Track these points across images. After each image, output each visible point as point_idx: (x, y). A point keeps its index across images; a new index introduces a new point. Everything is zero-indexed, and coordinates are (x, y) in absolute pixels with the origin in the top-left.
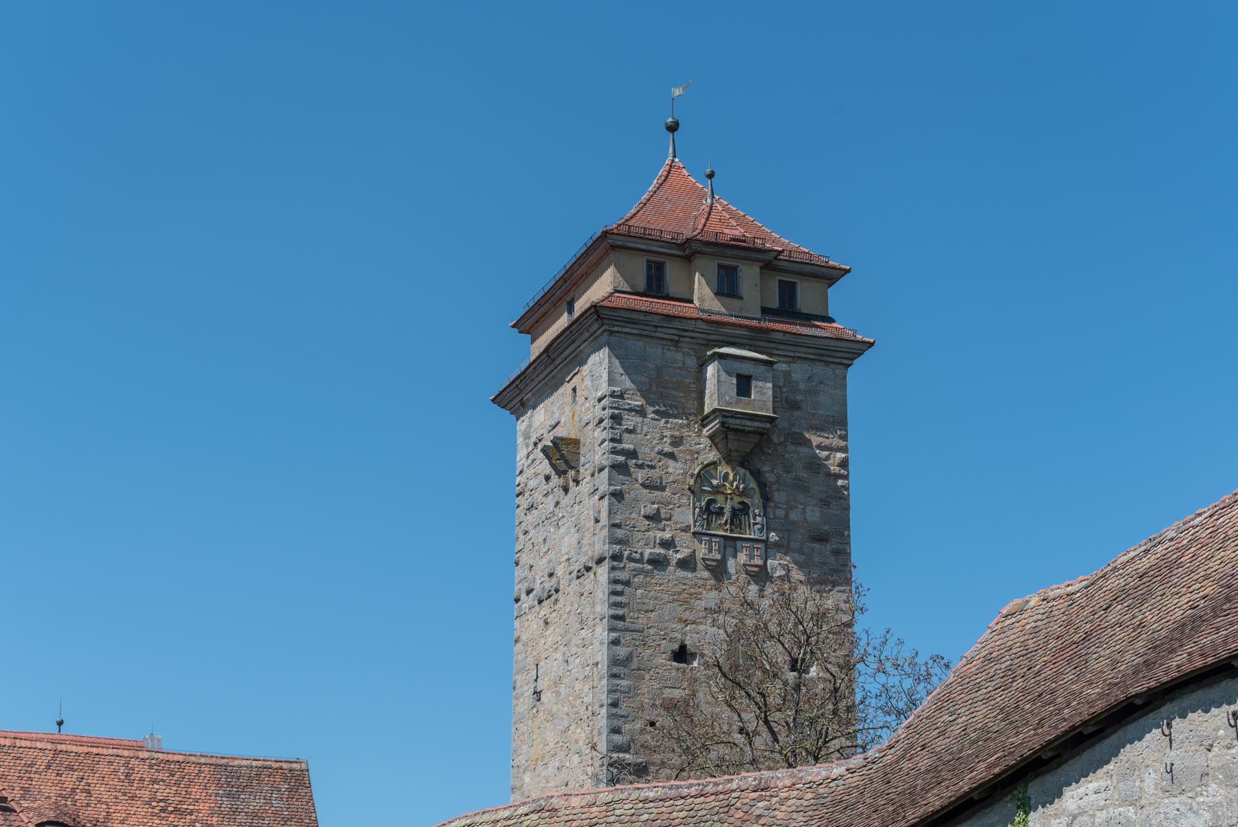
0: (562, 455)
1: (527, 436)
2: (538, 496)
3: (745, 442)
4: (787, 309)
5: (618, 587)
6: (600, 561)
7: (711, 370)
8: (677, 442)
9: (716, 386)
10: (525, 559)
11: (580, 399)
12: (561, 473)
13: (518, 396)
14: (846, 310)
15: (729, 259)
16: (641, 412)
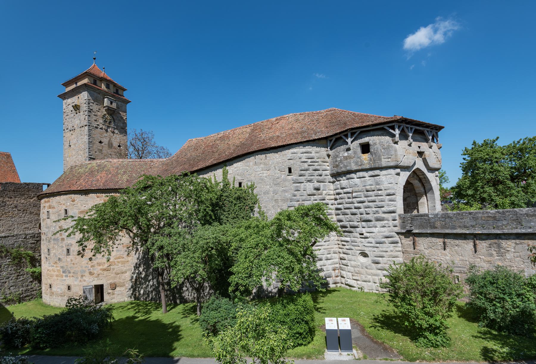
0: (76, 108)
1: (66, 103)
2: (69, 114)
3: (111, 111)
4: (117, 92)
5: (90, 130)
6: (86, 126)
7: (106, 99)
8: (99, 109)
9: (106, 102)
10: (65, 123)
11: (80, 99)
12: (75, 110)
13: (64, 96)
14: (126, 95)
15: (109, 83)
16: (93, 103)
